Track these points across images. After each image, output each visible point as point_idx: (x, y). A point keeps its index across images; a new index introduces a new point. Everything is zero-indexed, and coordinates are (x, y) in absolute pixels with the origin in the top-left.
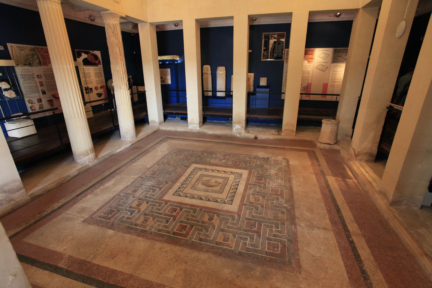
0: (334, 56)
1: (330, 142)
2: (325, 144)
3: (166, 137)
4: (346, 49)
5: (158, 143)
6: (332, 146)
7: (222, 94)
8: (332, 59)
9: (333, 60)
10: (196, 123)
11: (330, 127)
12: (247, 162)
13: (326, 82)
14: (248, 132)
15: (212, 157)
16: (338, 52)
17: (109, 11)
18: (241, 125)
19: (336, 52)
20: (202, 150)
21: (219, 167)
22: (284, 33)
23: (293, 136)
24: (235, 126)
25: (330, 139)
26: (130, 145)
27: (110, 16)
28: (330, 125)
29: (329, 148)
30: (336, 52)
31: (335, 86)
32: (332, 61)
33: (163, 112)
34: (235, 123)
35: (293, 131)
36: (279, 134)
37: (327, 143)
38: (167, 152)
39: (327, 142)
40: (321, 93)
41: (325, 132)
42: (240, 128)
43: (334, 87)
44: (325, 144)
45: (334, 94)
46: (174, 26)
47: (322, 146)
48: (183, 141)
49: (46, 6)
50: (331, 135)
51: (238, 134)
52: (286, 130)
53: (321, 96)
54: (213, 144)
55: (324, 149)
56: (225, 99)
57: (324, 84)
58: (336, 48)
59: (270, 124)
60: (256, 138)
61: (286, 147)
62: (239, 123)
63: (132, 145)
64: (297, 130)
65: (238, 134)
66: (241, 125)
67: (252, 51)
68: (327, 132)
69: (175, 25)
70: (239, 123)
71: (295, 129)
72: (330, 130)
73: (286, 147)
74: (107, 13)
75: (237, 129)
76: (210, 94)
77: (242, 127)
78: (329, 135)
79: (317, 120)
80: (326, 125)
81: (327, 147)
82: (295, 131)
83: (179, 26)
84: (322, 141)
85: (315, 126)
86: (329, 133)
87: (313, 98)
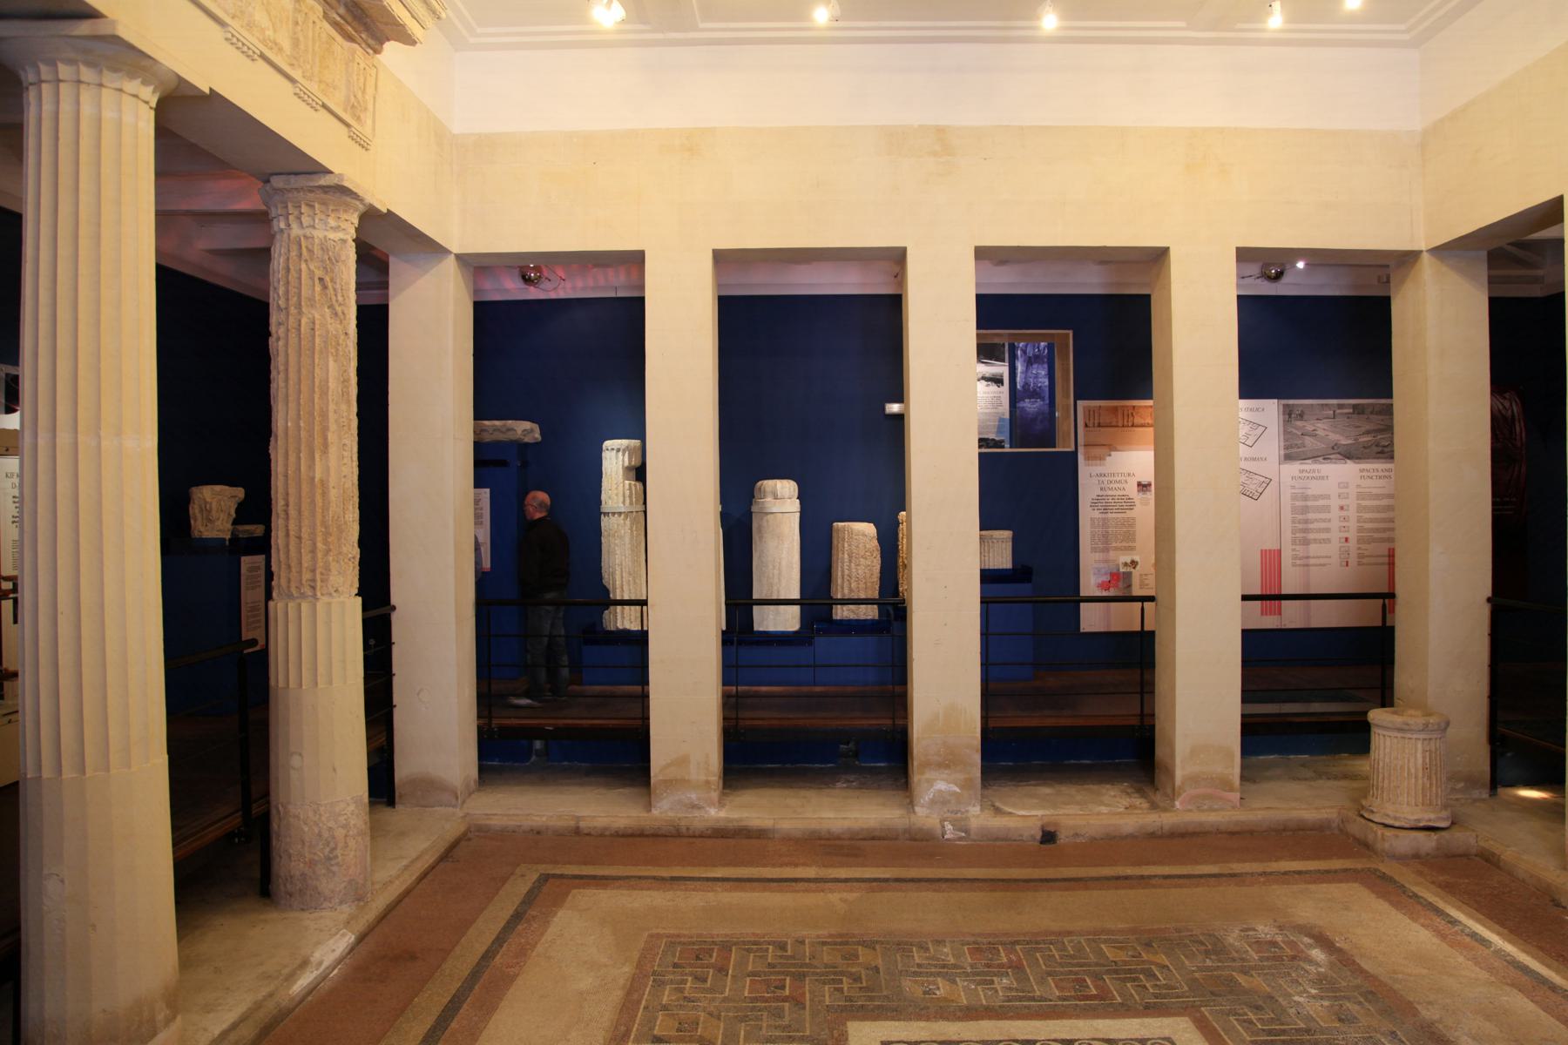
0: (1285, 432)
1: (1432, 816)
2: (1412, 829)
3: (545, 878)
4: (1326, 405)
5: (517, 917)
6: (1443, 833)
7: (787, 620)
8: (1282, 444)
9: (1286, 448)
10: (703, 778)
11: (1420, 745)
12: (1135, 971)
13: (1271, 545)
14: (998, 811)
15: (919, 966)
16: (1301, 416)
17: (328, 177)
18: (961, 776)
19: (1290, 415)
20: (825, 932)
21: (1011, 1018)
22: (1068, 334)
23: (1228, 812)
24: (931, 782)
25: (1430, 804)
26: (350, 938)
27: (324, 203)
28: (1422, 736)
29: (1438, 849)
30: (1290, 415)
31: (1312, 561)
32: (1282, 452)
33: (480, 729)
34: (927, 765)
35: (1226, 784)
36: (1154, 806)
37: (1421, 824)
38: (628, 969)
39: (1419, 820)
40: (1258, 592)
41: (1402, 768)
42: (955, 793)
43: (1307, 565)
44: (1412, 829)
45: (1313, 592)
46: (520, 284)
47: (1405, 843)
48: (669, 895)
49: (87, 110)
50: (1430, 784)
51: (949, 827)
52: (1194, 780)
53: (1258, 603)
54: (855, 895)
55: (1416, 856)
56: (811, 644)
57: (1264, 553)
58: (1291, 402)
59: (1066, 762)
60: (1048, 837)
61: (1237, 867)
62: (947, 767)
63: (361, 939)
64: (1243, 778)
65: (949, 827)
66: (961, 776)
67: (884, 409)
68: (1413, 771)
69: (527, 280)
70: (948, 762)
71: (1237, 770)
72: (1424, 758)
73: (1237, 867)
74: (312, 184)
75: (940, 801)
76: (787, 620)
77: (966, 785)
78: (1420, 782)
79: (1313, 719)
80: (1399, 735)
81: (1427, 842)
82: (1237, 781)
83: (545, 285)
84: (1396, 818)
85: (1334, 749)
86: (1420, 775)
87: (1292, 616)
